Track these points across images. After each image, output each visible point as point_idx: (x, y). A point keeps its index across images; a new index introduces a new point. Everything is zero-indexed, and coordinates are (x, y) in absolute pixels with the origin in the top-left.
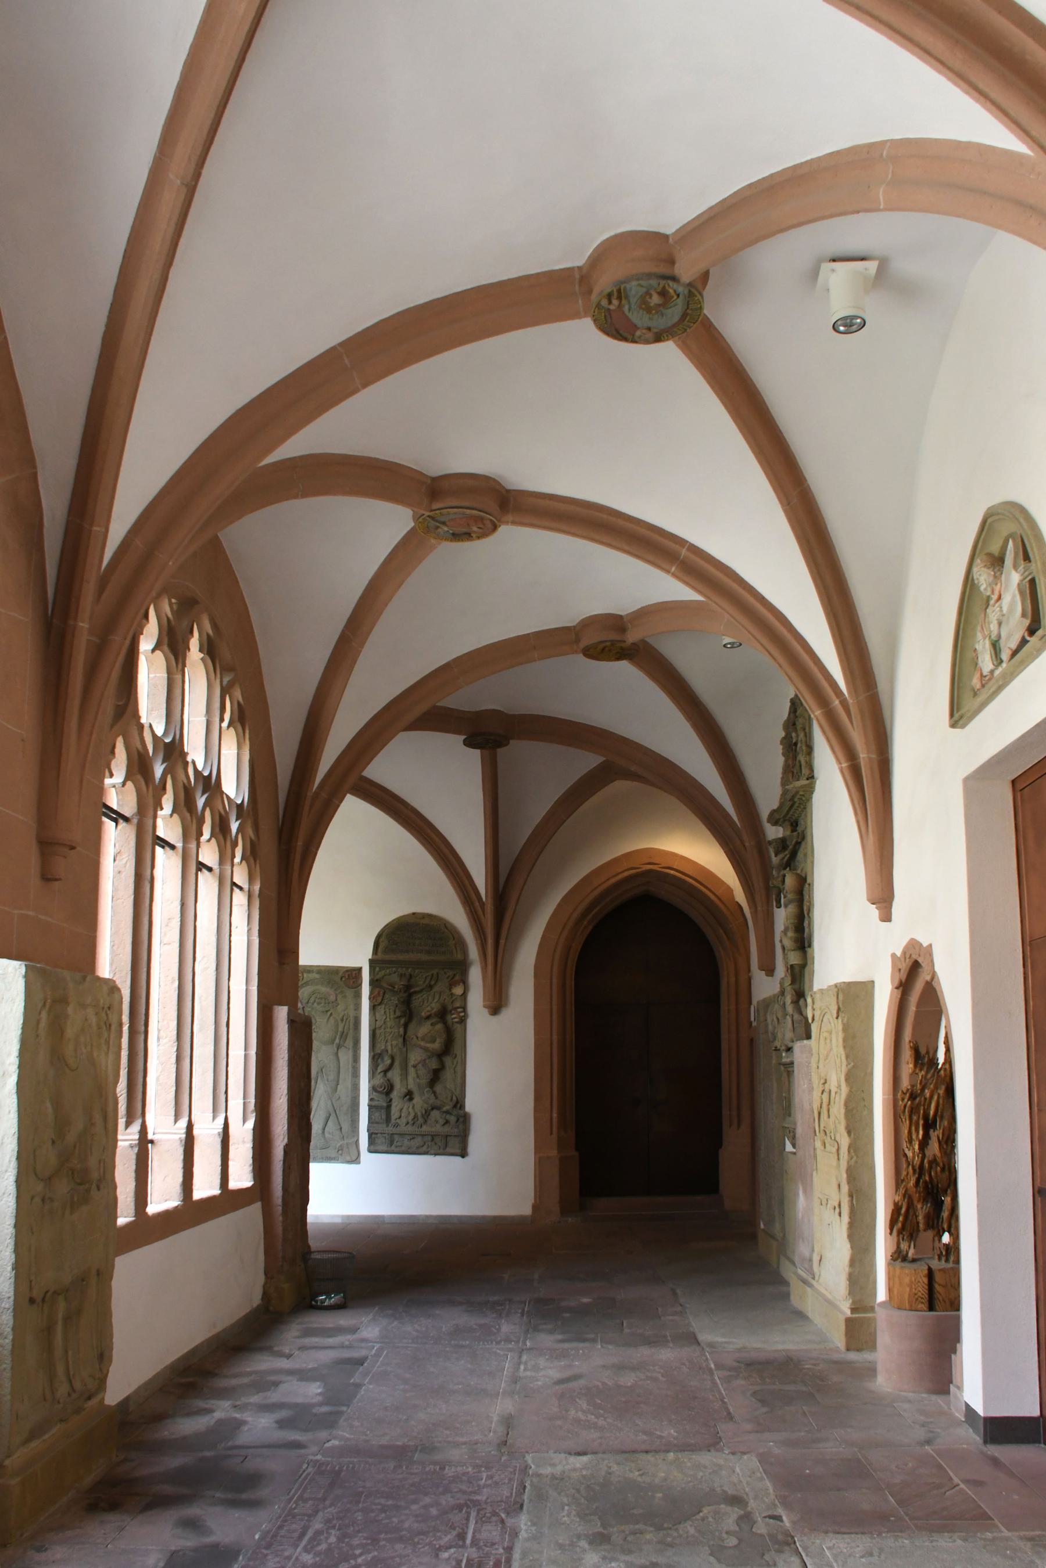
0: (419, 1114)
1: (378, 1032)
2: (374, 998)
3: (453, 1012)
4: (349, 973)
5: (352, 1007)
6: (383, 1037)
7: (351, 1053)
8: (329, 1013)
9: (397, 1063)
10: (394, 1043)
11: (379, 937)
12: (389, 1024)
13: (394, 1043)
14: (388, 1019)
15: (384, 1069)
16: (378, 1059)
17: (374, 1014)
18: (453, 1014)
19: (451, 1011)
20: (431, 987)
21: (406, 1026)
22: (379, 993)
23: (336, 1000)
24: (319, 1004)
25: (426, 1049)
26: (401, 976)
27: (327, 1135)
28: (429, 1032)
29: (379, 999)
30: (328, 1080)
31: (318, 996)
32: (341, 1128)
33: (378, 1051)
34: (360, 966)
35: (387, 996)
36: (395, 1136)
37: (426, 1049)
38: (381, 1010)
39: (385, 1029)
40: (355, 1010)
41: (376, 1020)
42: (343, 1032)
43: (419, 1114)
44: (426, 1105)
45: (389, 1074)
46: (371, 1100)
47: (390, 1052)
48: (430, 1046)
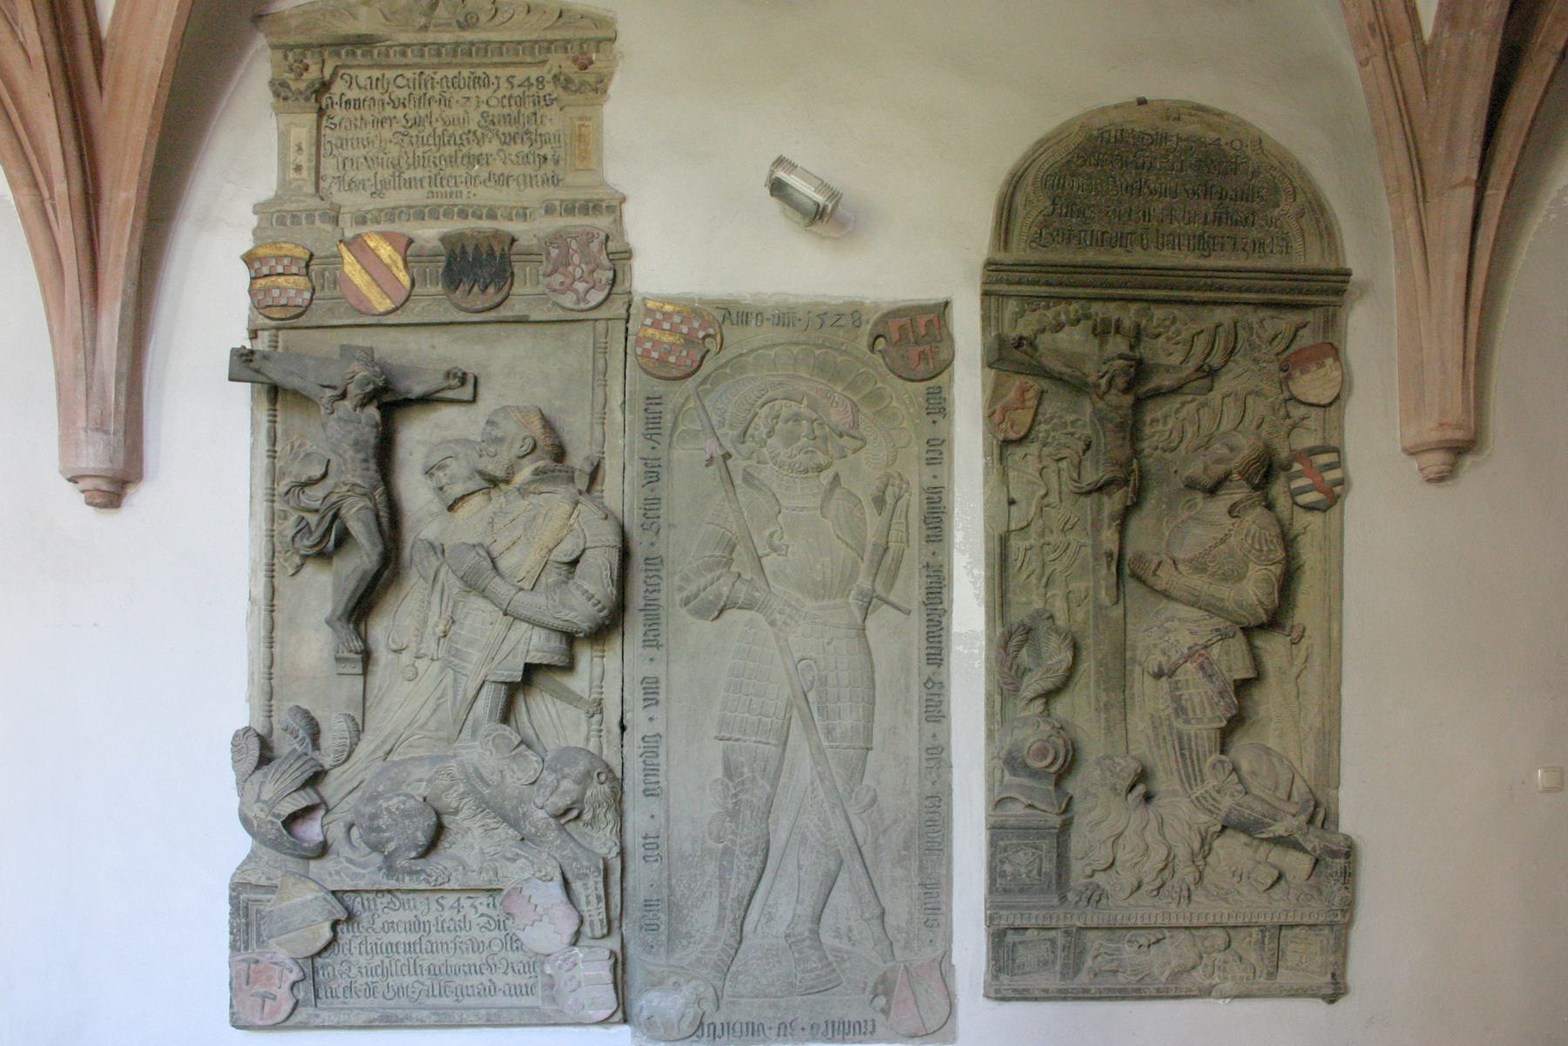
0: (1182, 852)
1: (1016, 544)
2: (1005, 409)
3: (1297, 467)
4: (905, 320)
5: (917, 449)
6: (1035, 565)
7: (916, 624)
8: (826, 478)
9: (1088, 666)
10: (1078, 586)
11: (1015, 183)
12: (1056, 516)
13: (1078, 586)
14: (1053, 498)
15: (1048, 685)
16: (1020, 647)
17: (1004, 475)
18: (1299, 475)
19: (1287, 467)
20: (1209, 374)
21: (1123, 519)
22: (1023, 391)
23: (856, 425)
24: (791, 439)
25: (1211, 608)
26: (1102, 331)
27: (827, 938)
28: (1223, 541)
29: (1025, 417)
30: (829, 731)
31: (785, 413)
32: (883, 913)
33: (1018, 615)
34: (940, 297)
35: (1048, 408)
36: (1091, 935)
37: (1211, 608)
38: (1026, 461)
39: (1042, 535)
40: (931, 462)
41: (1012, 502)
42: (886, 549)
43: (1182, 852)
44: (1204, 818)
45: (1061, 707)
46: (998, 803)
47: (1061, 621)
48: (1226, 593)
